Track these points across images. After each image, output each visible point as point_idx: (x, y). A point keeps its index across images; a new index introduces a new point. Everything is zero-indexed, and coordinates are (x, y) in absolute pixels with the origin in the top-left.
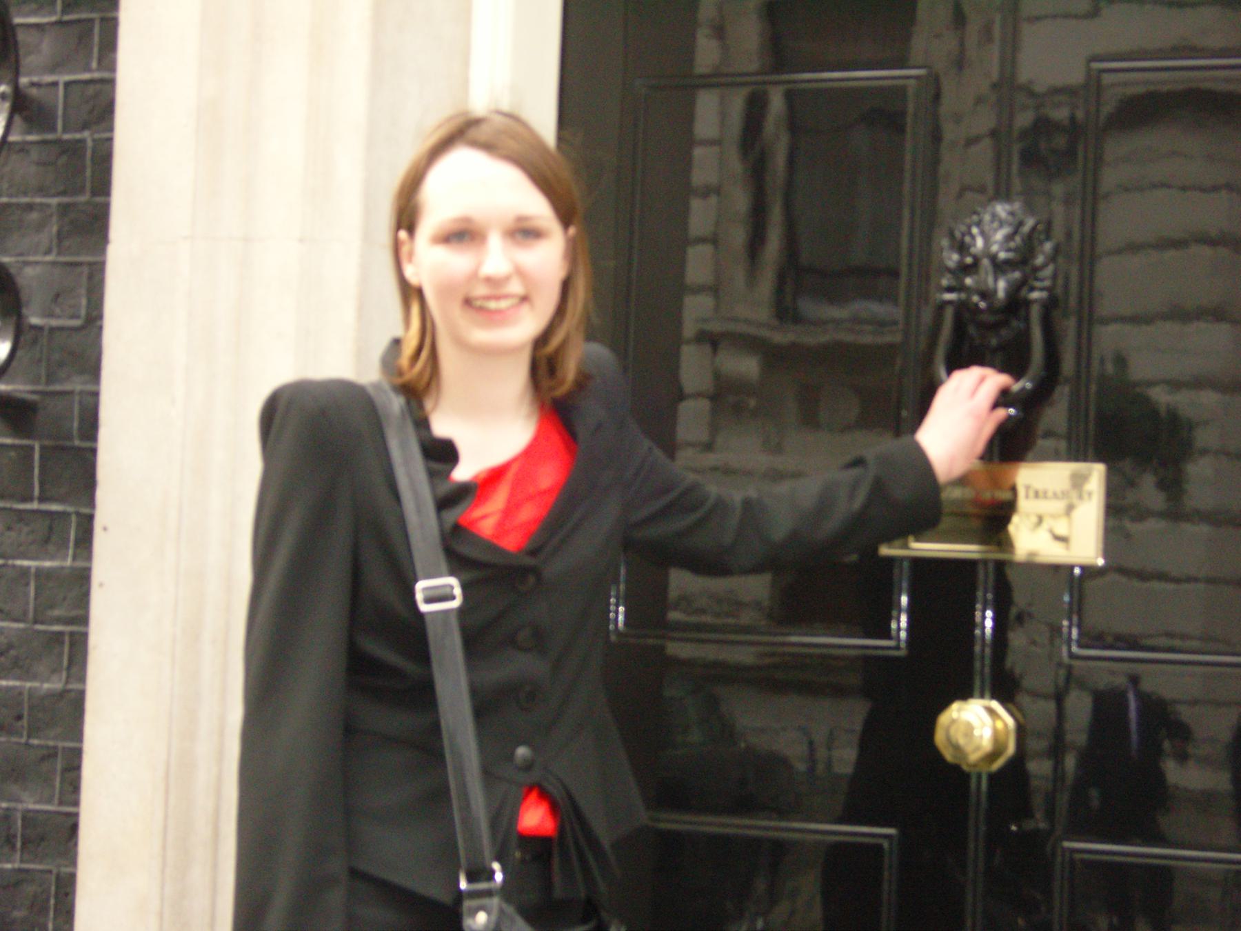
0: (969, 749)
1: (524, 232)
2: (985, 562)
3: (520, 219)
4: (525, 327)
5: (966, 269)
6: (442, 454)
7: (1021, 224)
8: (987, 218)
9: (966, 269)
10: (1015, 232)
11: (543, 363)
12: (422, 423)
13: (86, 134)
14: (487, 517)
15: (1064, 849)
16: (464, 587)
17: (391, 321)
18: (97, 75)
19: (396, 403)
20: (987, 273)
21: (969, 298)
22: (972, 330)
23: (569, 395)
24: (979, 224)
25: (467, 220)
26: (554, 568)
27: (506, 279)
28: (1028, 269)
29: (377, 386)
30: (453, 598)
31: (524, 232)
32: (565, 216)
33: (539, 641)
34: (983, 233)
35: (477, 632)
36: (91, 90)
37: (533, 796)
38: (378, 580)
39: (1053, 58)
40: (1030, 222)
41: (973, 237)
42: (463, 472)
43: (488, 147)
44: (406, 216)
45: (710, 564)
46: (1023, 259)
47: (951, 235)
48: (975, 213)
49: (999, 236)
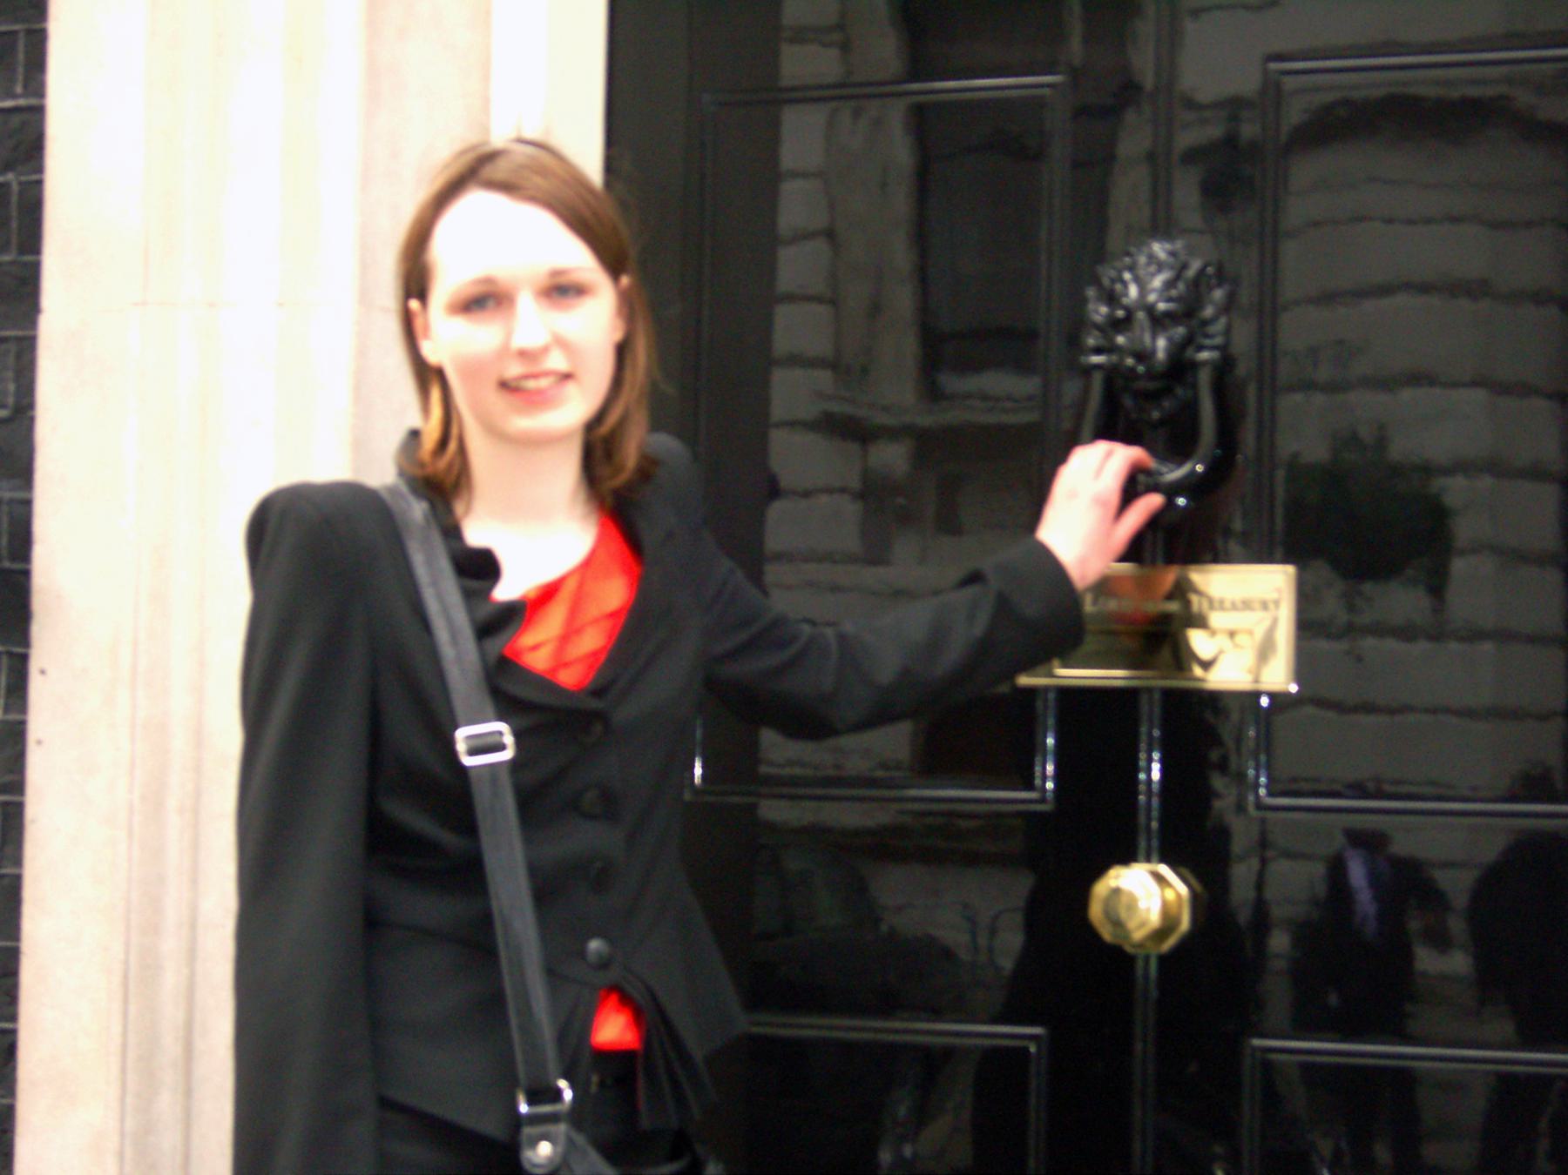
0: (1132, 924)
2: (1150, 690)
5: (1118, 325)
6: (480, 568)
7: (1185, 267)
8: (1142, 260)
9: (1118, 325)
12: (452, 532)
13: (10, 176)
14: (538, 645)
15: (1254, 1049)
18: (22, 102)
19: (417, 510)
20: (1143, 330)
21: (1122, 360)
22: (1128, 401)
24: (1131, 269)
26: (625, 713)
28: (1194, 322)
29: (392, 490)
33: (609, 806)
34: (1137, 280)
36: (16, 120)
40: (1195, 266)
41: (1125, 284)
42: (504, 592)
46: (1187, 311)
48: (1128, 254)
49: (1157, 282)
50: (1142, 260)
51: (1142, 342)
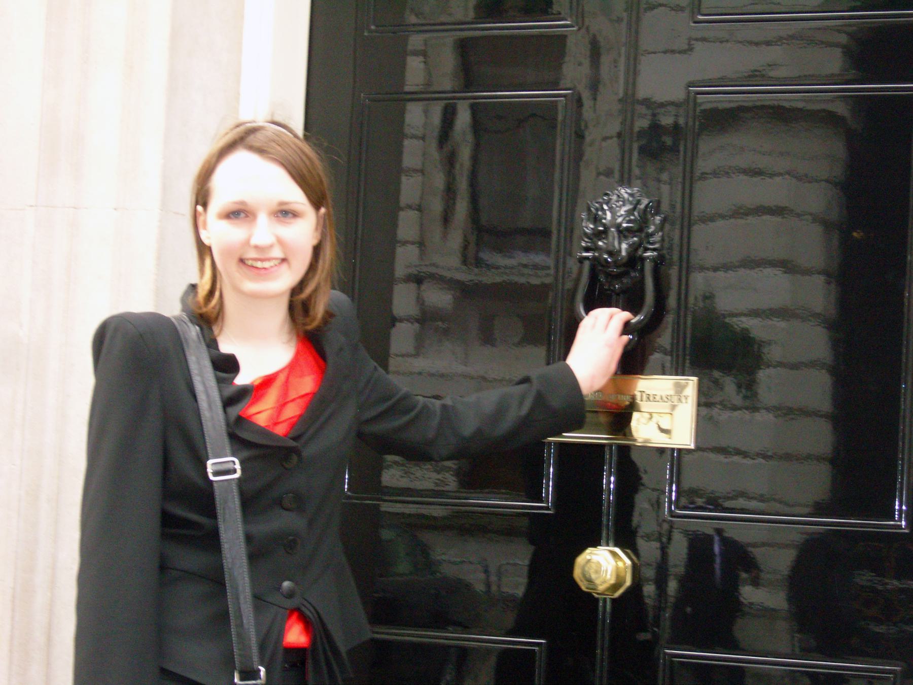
0: (598, 582)
1: (285, 213)
2: (611, 445)
3: (282, 203)
4: (284, 280)
5: (599, 235)
6: (227, 366)
7: (639, 202)
9: (599, 235)
10: (635, 209)
11: (298, 305)
12: (212, 344)
16: (242, 463)
17: (189, 271)
19: (193, 331)
20: (614, 239)
21: (600, 255)
22: (602, 278)
23: (318, 329)
24: (607, 204)
25: (243, 203)
26: (309, 451)
27: (271, 246)
28: (643, 235)
29: (179, 319)
30: (235, 471)
31: (285, 213)
32: (317, 201)
34: (611, 209)
35: (252, 499)
37: (294, 617)
38: (181, 458)
39: (664, 81)
40: (645, 201)
42: (242, 379)
43: (261, 151)
44: (202, 197)
45: (416, 454)
46: (639, 228)
47: (589, 210)
48: (606, 194)
49: (622, 211)
50: (615, 198)
51: (614, 246)
